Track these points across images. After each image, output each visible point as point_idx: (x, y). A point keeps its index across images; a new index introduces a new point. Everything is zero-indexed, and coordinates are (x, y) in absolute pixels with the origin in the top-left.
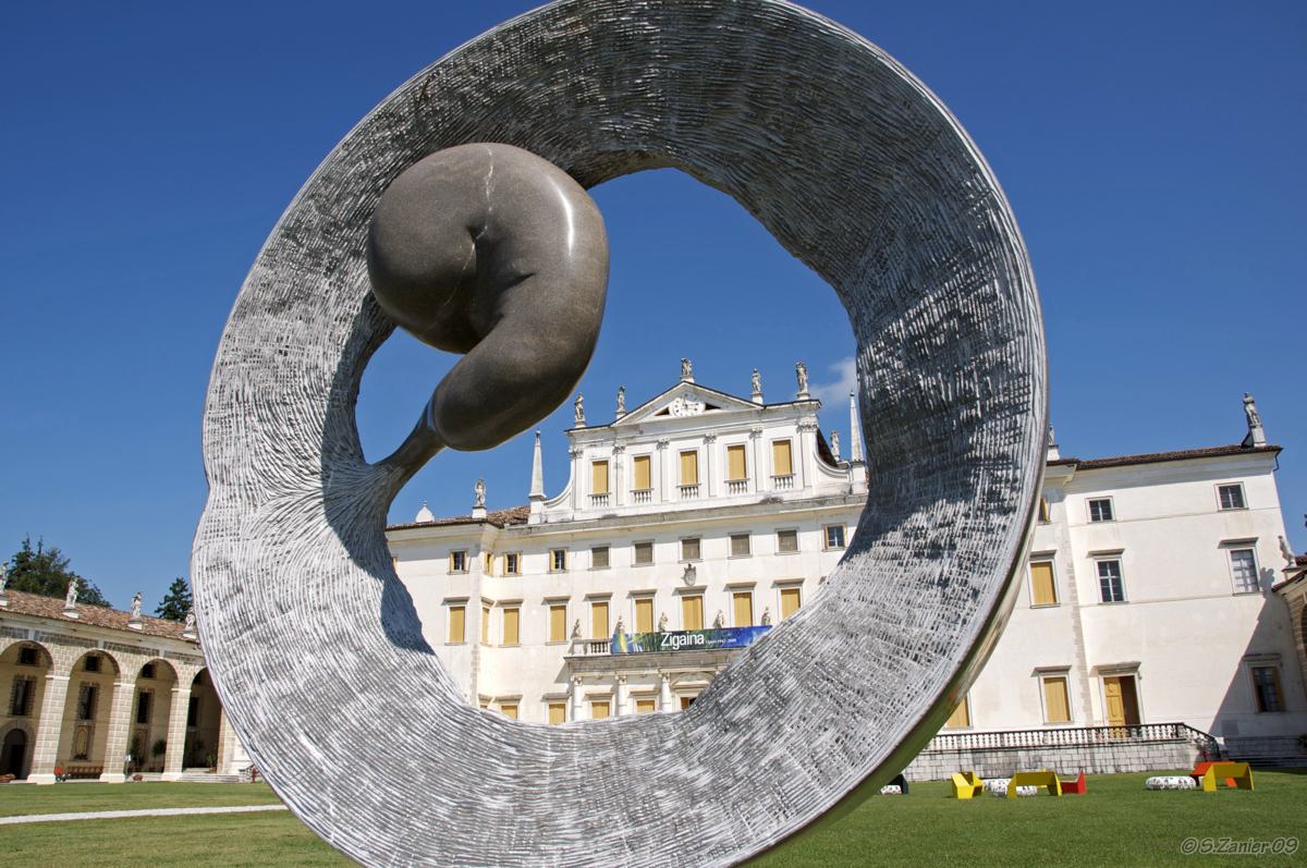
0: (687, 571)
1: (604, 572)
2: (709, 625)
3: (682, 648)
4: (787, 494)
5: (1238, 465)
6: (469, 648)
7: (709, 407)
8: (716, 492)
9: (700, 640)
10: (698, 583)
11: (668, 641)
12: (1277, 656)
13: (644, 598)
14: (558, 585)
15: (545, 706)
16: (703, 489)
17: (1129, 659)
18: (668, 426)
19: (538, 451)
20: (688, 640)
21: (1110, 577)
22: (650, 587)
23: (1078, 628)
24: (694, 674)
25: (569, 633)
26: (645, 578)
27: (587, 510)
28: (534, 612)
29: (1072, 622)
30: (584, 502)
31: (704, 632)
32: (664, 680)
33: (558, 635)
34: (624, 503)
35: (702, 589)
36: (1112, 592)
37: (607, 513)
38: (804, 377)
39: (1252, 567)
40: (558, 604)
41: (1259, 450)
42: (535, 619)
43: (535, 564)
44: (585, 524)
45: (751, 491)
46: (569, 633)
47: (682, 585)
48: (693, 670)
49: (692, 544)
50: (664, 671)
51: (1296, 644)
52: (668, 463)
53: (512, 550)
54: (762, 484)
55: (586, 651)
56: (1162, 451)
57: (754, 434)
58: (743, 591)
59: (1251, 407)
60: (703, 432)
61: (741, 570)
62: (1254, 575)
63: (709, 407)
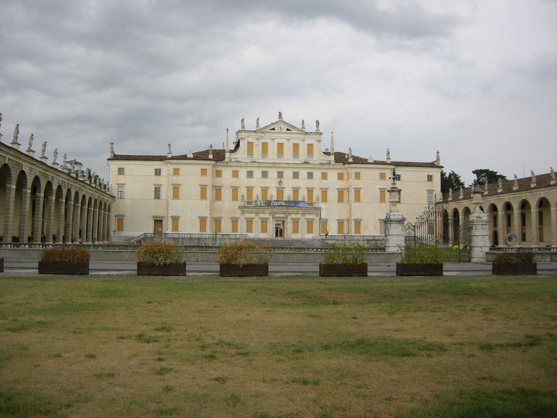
1: (252, 179)
2: (285, 199)
3: (278, 206)
9: (283, 204)
10: (283, 186)
20: (279, 203)
28: (227, 191)
31: (285, 201)
33: (235, 198)
35: (284, 188)
40: (235, 190)
47: (278, 186)
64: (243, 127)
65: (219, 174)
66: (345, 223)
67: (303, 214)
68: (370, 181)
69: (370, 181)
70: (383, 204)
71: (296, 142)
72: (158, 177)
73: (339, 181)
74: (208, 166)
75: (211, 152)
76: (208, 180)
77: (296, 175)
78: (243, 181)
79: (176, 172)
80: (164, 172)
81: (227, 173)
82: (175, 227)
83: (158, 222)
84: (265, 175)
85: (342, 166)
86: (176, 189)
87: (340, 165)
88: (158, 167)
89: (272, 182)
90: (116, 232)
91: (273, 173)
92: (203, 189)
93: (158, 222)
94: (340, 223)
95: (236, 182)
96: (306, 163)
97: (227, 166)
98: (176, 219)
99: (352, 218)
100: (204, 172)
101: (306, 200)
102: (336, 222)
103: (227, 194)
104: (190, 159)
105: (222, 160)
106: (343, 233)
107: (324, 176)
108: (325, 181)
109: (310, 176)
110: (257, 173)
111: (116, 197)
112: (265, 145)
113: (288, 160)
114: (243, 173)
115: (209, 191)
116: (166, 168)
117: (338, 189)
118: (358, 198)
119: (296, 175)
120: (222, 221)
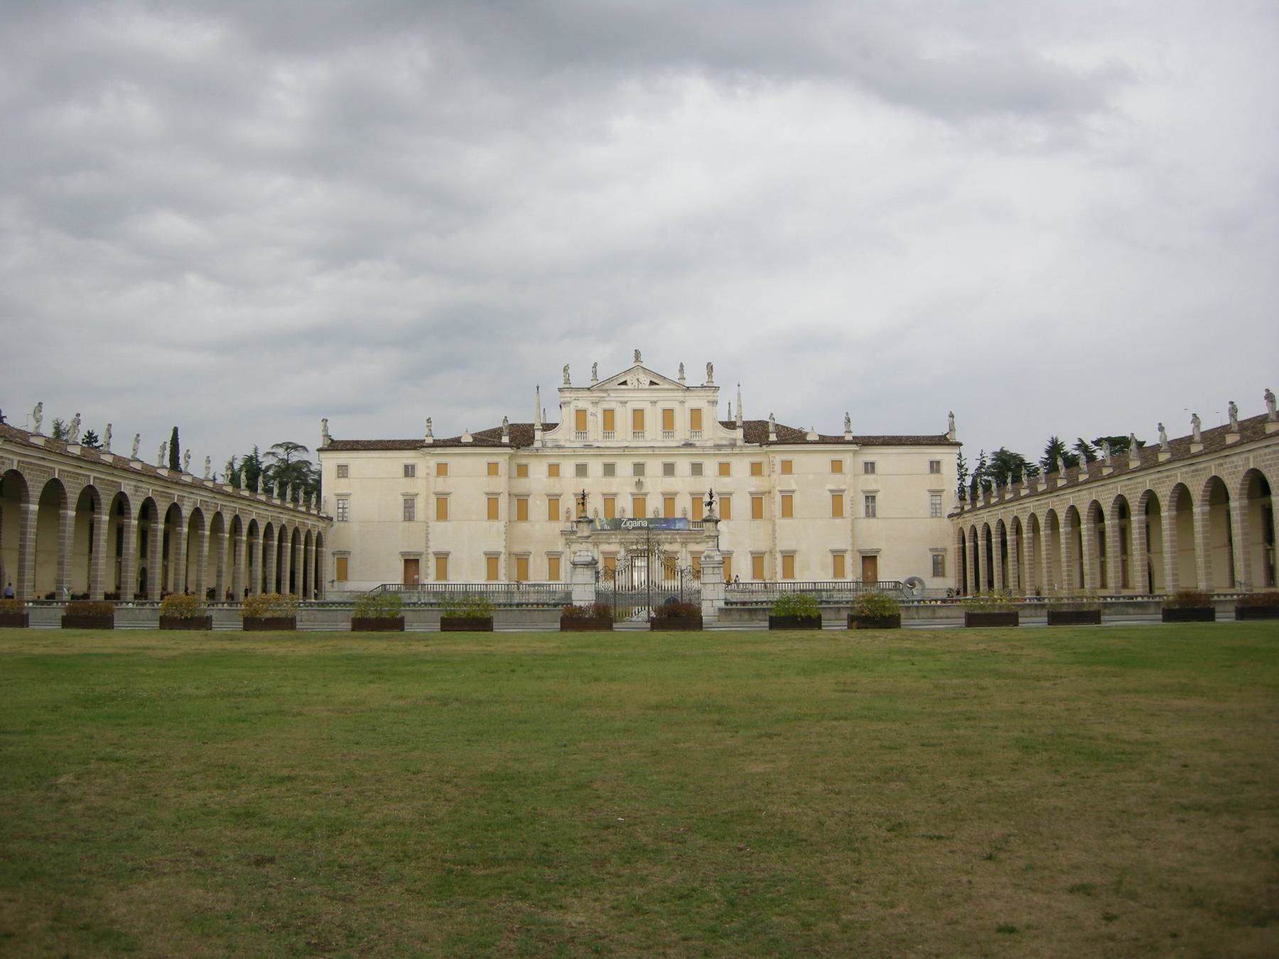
2: (650, 515)
9: (645, 524)
10: (644, 491)
12: (945, 550)
20: (637, 524)
33: (553, 515)
35: (646, 494)
40: (554, 500)
45: (677, 438)
64: (567, 381)
65: (523, 471)
66: (766, 558)
67: (684, 544)
68: (811, 477)
69: (811, 477)
70: (838, 521)
71: (668, 405)
72: (409, 480)
73: (754, 478)
74: (501, 457)
75: (506, 431)
76: (500, 484)
77: (669, 469)
78: (569, 484)
79: (442, 470)
80: (421, 470)
81: (538, 469)
82: (442, 572)
83: (411, 563)
84: (609, 470)
85: (758, 450)
86: (442, 501)
87: (754, 448)
88: (409, 462)
89: (623, 484)
90: (336, 584)
91: (624, 467)
92: (493, 500)
93: (411, 563)
94: (757, 558)
95: (554, 486)
96: (688, 445)
97: (537, 455)
98: (442, 558)
99: (778, 549)
100: (493, 469)
101: (690, 517)
102: (749, 557)
103: (538, 508)
105: (528, 445)
106: (762, 577)
107: (724, 470)
108: (726, 480)
109: (697, 469)
110: (595, 467)
112: (609, 415)
113: (653, 440)
114: (568, 468)
115: (503, 503)
116: (425, 463)
117: (751, 494)
118: (787, 511)
119: (669, 469)
120: (531, 560)
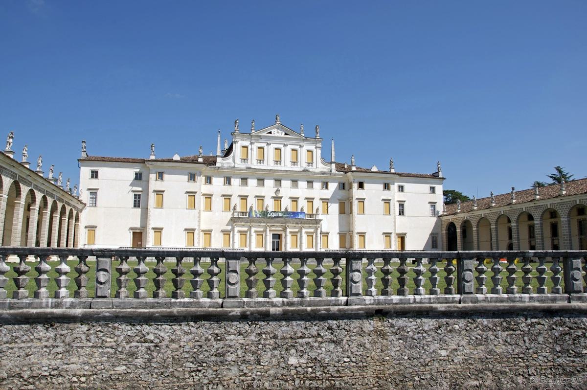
0: (277, 191)
1: (246, 188)
2: (283, 210)
3: (275, 217)
4: (311, 169)
5: (433, 181)
6: (197, 211)
7: (286, 134)
8: (287, 165)
9: (281, 215)
10: (280, 195)
11: (270, 214)
13: (261, 198)
14: (227, 190)
15: (222, 234)
16: (282, 163)
17: (404, 232)
18: (269, 139)
19: (219, 138)
20: (277, 215)
21: (401, 208)
22: (263, 195)
23: (395, 222)
24: (277, 226)
25: (232, 208)
26: (261, 191)
27: (239, 164)
28: (218, 199)
29: (393, 220)
30: (238, 161)
31: (283, 212)
32: (268, 227)
33: (228, 208)
34: (255, 165)
35: (281, 198)
36: (402, 213)
37: (248, 166)
38: (318, 130)
39: (435, 209)
40: (228, 197)
41: (440, 178)
42: (218, 202)
43: (218, 181)
44: (241, 169)
46: (232, 208)
47: (274, 195)
48: (278, 225)
49: (278, 181)
50: (268, 224)
51: (442, 231)
52: (270, 152)
53: (209, 175)
54: (302, 165)
55: (238, 215)
56: (413, 173)
57: (301, 147)
58: (295, 200)
59: (439, 166)
60: (284, 143)
61: (295, 193)
62: (435, 212)
63: (286, 134)
82: (159, 240)
101: (305, 211)
104: (176, 161)
111: (87, 205)
